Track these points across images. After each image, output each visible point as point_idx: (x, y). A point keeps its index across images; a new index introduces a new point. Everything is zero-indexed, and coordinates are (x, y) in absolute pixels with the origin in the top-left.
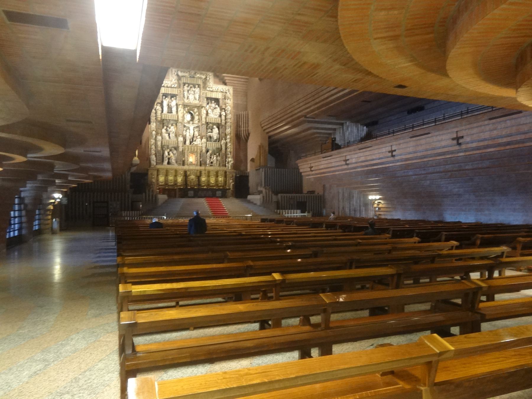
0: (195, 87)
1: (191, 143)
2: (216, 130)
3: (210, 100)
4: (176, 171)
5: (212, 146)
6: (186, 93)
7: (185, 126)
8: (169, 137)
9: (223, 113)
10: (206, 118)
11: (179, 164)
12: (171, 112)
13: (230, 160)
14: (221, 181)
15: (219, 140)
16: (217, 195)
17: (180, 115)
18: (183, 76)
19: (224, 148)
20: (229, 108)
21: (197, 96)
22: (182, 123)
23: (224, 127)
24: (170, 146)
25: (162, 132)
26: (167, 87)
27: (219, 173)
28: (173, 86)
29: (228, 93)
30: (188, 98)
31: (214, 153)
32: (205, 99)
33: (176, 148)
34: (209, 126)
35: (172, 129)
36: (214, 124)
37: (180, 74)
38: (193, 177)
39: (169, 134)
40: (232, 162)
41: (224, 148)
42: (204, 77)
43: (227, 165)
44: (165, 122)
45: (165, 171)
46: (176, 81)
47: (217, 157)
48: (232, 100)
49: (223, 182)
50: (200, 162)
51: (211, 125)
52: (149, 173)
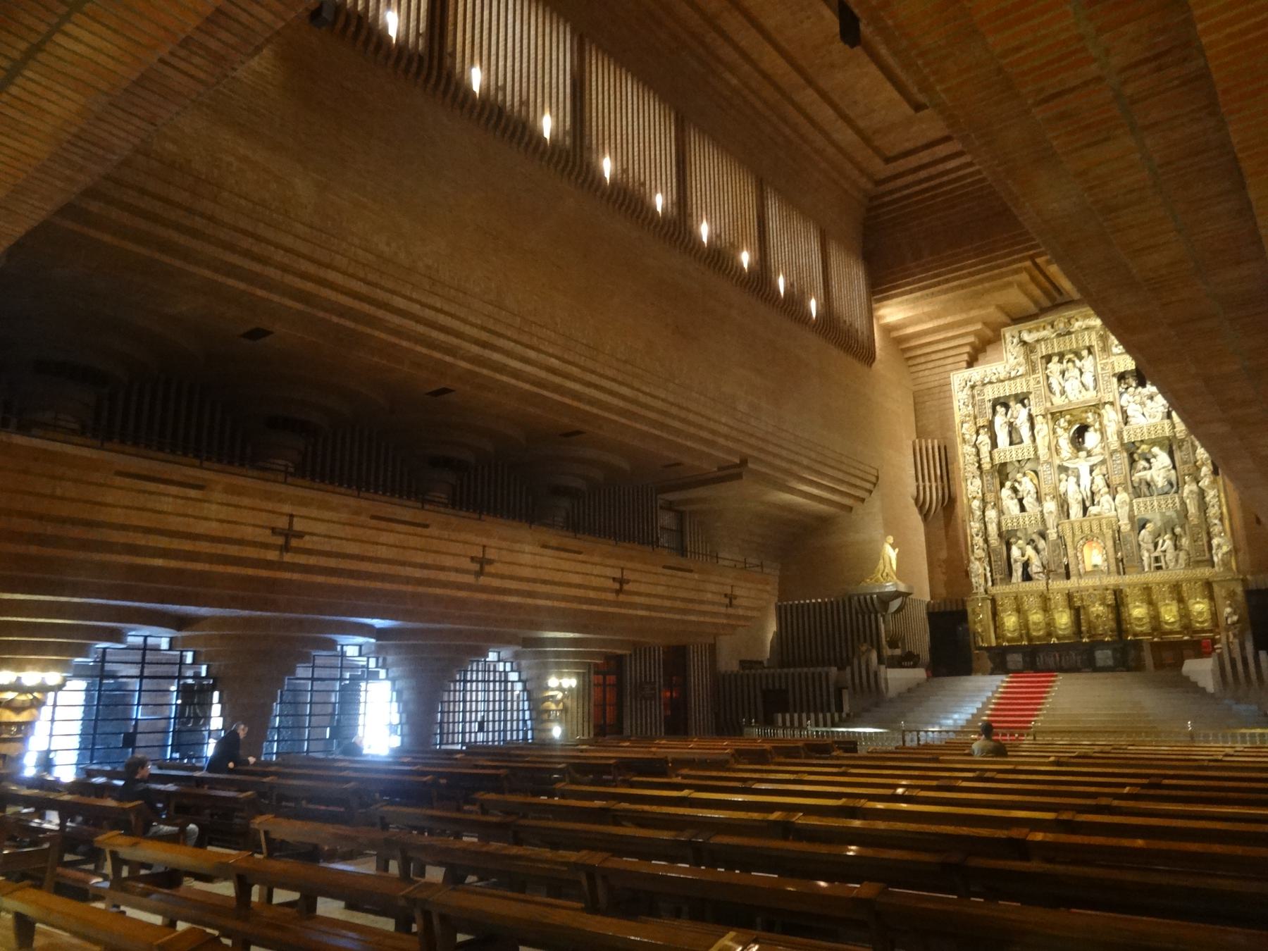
0: (1081, 358)
1: (1085, 510)
2: (1162, 459)
5: (1155, 510)
6: (1055, 381)
7: (1063, 469)
8: (1023, 509)
10: (1120, 434)
11: (1058, 575)
12: (1022, 442)
13: (1222, 545)
14: (1201, 613)
15: (1175, 486)
16: (1100, 663)
17: (1042, 442)
18: (1038, 341)
19: (1192, 509)
21: (1088, 379)
22: (1050, 464)
24: (1030, 532)
25: (999, 499)
27: (1185, 588)
28: (1013, 374)
30: (1063, 392)
31: (1168, 527)
32: (1115, 380)
33: (1043, 535)
34: (1133, 453)
35: (1027, 486)
36: (1153, 443)
37: (1027, 337)
38: (1097, 609)
39: (1021, 501)
40: (1225, 549)
41: (1192, 509)
44: (1009, 468)
47: (1176, 538)
49: (1206, 616)
50: (1119, 561)
51: (1144, 447)
52: (969, 610)
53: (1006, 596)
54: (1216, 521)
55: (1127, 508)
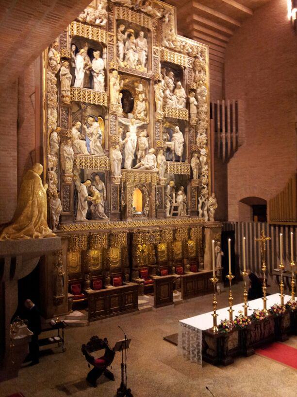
3: (168, 67)
4: (111, 236)
9: (192, 99)
10: (164, 108)
20: (204, 90)
23: (193, 131)
26: (85, 23)
28: (98, 22)
29: (201, 59)
42: (159, 15)
43: (200, 211)
45: (85, 239)
46: (104, 11)
48: (208, 74)
53: (78, 234)
54: (205, 186)
55: (165, 167)
